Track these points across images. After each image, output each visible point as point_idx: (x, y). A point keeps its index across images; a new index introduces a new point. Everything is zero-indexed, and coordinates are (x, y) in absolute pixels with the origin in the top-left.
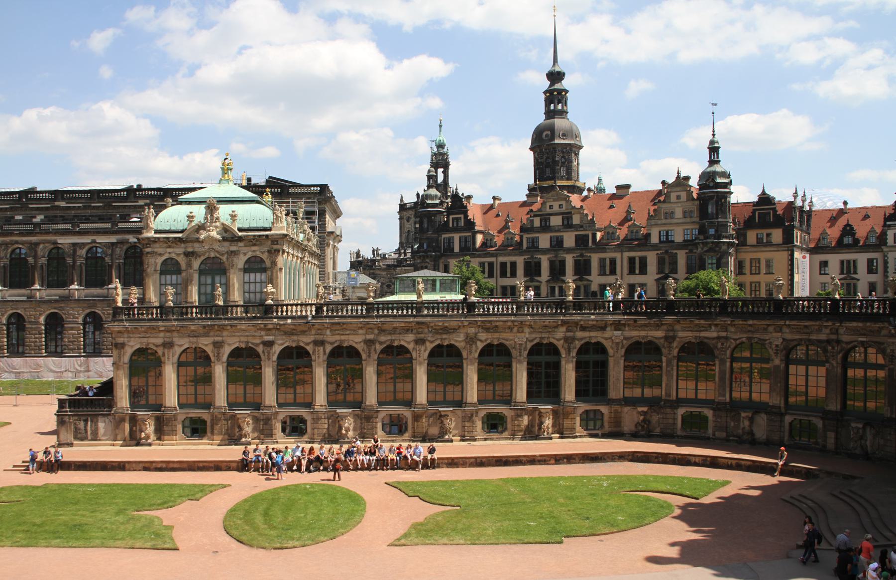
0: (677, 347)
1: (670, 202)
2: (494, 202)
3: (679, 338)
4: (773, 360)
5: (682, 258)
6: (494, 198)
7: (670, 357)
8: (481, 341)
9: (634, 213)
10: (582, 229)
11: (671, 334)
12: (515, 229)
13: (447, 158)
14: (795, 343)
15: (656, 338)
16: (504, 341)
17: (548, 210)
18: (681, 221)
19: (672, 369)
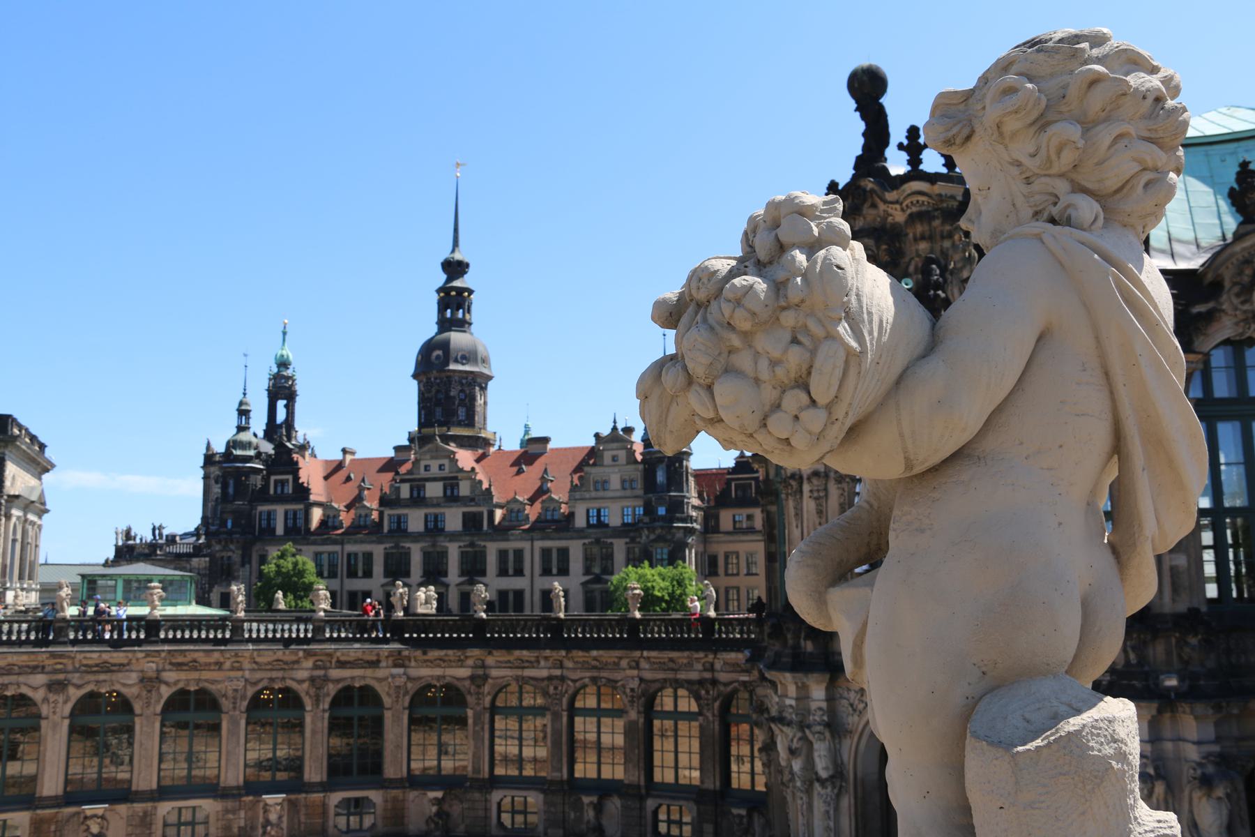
0: (489, 693)
1: (602, 465)
2: (344, 458)
3: (492, 678)
4: (627, 712)
5: (619, 547)
6: (344, 451)
7: (478, 708)
8: (167, 684)
9: (552, 481)
10: (473, 504)
11: (480, 672)
12: (372, 503)
13: (292, 384)
14: (657, 685)
15: (458, 679)
16: (206, 685)
17: (422, 473)
18: (618, 494)
19: (483, 729)
